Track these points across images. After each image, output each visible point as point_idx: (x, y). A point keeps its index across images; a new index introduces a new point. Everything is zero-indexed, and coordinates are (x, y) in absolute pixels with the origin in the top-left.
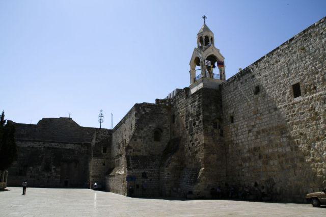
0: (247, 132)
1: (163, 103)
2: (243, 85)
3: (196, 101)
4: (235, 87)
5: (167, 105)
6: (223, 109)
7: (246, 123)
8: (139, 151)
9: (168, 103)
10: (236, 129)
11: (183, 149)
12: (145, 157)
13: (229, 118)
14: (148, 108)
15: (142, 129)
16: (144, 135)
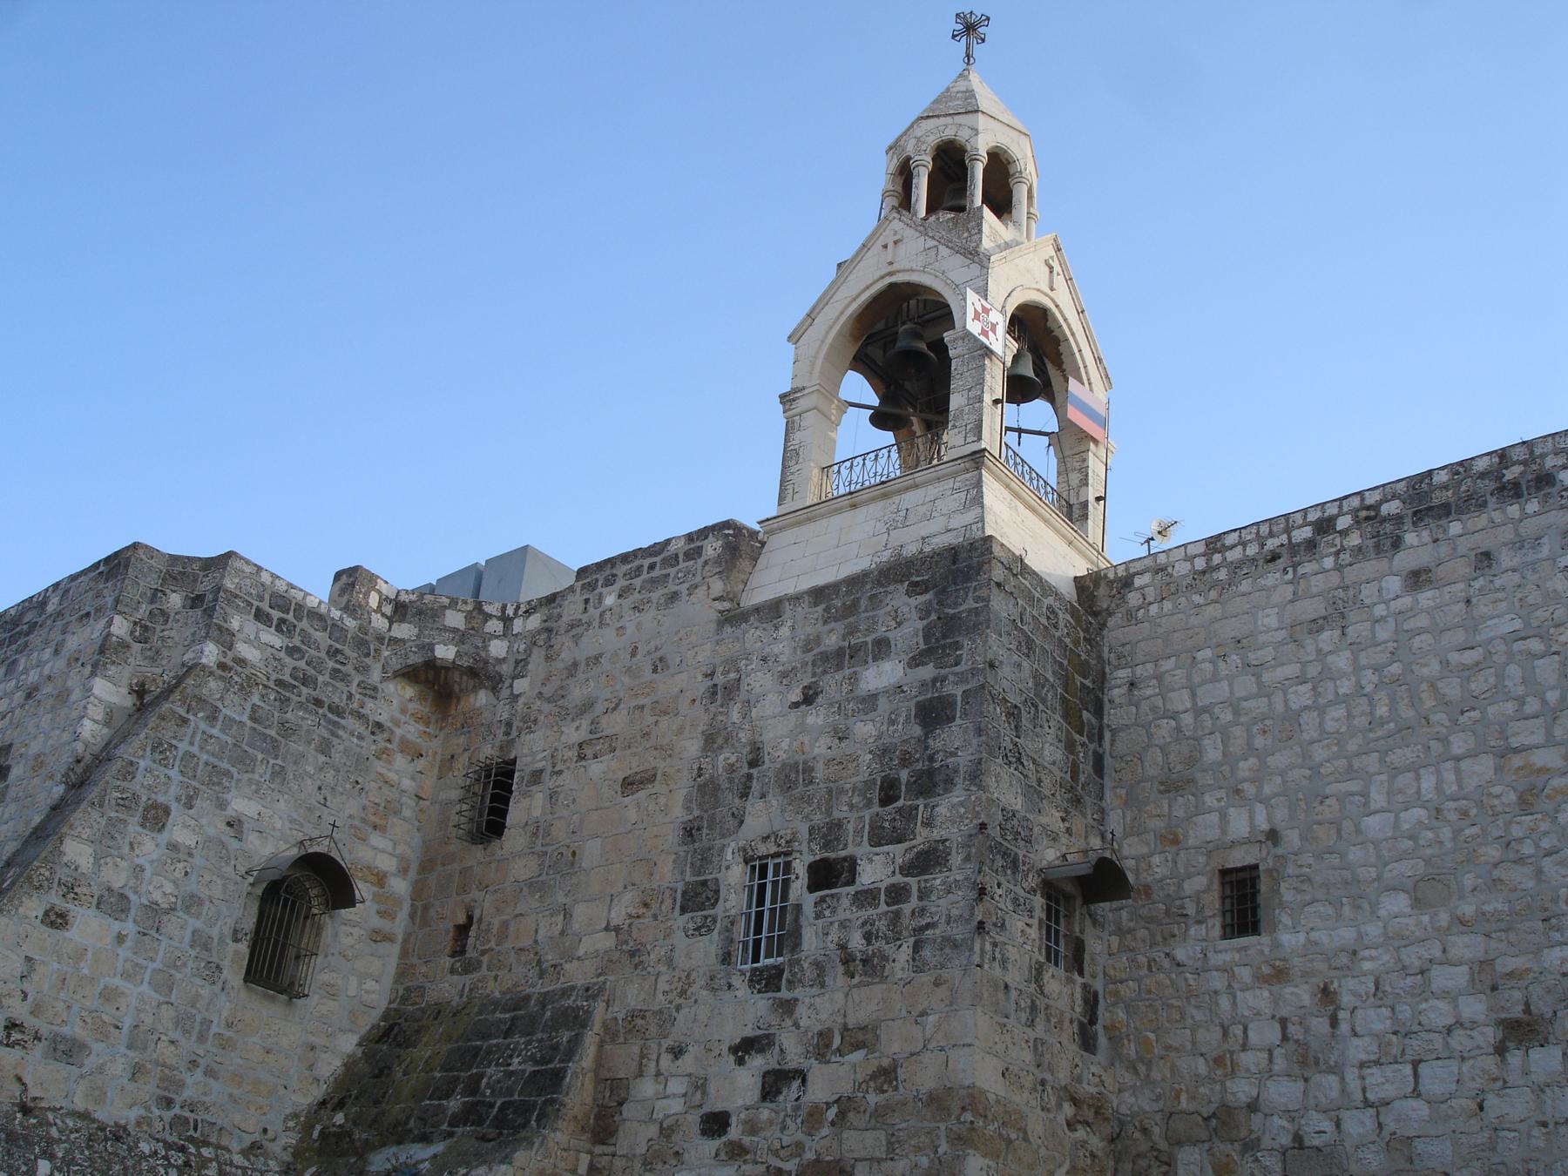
0: (1489, 1035)
1: (404, 631)
2: (1426, 598)
3: (882, 648)
4: (1313, 608)
5: (445, 652)
7: (1467, 946)
8: (67, 1051)
9: (460, 637)
10: (1300, 995)
11: (603, 1128)
12: (119, 1134)
13: (1199, 882)
14: (260, 616)
15: (156, 817)
16: (160, 890)
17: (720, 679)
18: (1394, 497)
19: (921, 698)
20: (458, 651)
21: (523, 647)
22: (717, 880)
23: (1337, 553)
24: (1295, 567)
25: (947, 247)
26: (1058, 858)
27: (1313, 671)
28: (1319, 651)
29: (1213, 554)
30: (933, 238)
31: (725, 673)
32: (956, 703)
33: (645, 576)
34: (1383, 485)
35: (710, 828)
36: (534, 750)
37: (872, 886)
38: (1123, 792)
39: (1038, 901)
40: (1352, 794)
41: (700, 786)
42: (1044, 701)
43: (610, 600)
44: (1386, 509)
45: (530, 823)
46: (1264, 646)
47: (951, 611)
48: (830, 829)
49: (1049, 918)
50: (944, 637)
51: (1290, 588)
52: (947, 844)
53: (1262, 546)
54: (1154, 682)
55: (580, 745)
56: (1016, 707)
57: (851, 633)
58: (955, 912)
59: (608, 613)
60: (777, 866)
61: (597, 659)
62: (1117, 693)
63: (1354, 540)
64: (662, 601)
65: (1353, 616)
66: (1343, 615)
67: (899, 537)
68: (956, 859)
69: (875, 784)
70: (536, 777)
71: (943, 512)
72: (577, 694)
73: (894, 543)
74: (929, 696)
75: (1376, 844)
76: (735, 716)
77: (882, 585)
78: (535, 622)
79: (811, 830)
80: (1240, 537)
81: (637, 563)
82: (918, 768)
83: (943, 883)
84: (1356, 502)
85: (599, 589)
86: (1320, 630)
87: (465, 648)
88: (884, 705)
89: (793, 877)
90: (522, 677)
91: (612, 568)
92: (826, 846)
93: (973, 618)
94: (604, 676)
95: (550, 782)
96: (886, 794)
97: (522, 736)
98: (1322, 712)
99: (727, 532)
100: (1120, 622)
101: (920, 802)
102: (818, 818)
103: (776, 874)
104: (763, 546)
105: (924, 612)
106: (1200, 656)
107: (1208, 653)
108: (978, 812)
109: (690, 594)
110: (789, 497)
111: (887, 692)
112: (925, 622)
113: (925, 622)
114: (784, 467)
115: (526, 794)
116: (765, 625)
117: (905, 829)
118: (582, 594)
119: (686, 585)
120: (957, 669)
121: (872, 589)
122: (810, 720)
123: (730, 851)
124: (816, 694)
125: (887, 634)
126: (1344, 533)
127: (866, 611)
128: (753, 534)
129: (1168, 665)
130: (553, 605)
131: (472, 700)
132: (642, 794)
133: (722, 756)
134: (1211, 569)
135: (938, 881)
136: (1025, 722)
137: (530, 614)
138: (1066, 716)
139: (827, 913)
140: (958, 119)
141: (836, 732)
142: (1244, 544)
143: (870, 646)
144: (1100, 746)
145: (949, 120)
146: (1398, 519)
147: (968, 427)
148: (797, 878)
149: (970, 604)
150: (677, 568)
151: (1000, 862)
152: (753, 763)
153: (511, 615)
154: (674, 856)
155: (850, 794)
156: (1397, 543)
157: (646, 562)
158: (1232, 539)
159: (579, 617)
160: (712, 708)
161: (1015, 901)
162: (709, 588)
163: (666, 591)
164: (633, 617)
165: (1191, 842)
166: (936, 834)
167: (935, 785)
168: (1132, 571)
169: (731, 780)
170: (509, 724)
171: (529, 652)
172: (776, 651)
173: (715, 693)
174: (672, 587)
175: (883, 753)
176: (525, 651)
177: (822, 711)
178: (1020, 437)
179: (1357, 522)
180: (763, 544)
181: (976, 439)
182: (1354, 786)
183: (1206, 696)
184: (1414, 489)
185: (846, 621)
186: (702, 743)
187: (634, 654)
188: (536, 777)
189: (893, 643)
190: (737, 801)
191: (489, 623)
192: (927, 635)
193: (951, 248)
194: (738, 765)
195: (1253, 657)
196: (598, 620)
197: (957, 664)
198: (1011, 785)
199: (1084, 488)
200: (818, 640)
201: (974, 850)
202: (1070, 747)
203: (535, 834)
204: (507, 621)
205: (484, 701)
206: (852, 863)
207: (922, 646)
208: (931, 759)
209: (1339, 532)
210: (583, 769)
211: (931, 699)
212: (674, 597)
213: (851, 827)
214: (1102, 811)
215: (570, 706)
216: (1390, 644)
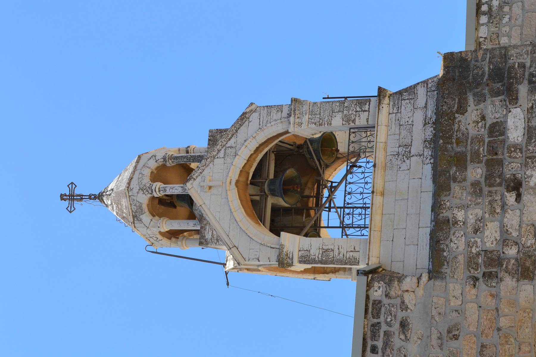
25: (230, 139)
30: (219, 151)
31: (477, 266)
67: (417, 147)
77: (452, 135)
109: (407, 308)
110: (356, 255)
111: (529, 119)
112: (488, 96)
113: (488, 96)
125: (487, 127)
134: (490, 13)
145: (137, 173)
147: (358, 109)
160: (501, 275)
162: (407, 291)
163: (397, 333)
172: (473, 221)
189: (495, 121)
197: (524, 67)
212: (404, 325)
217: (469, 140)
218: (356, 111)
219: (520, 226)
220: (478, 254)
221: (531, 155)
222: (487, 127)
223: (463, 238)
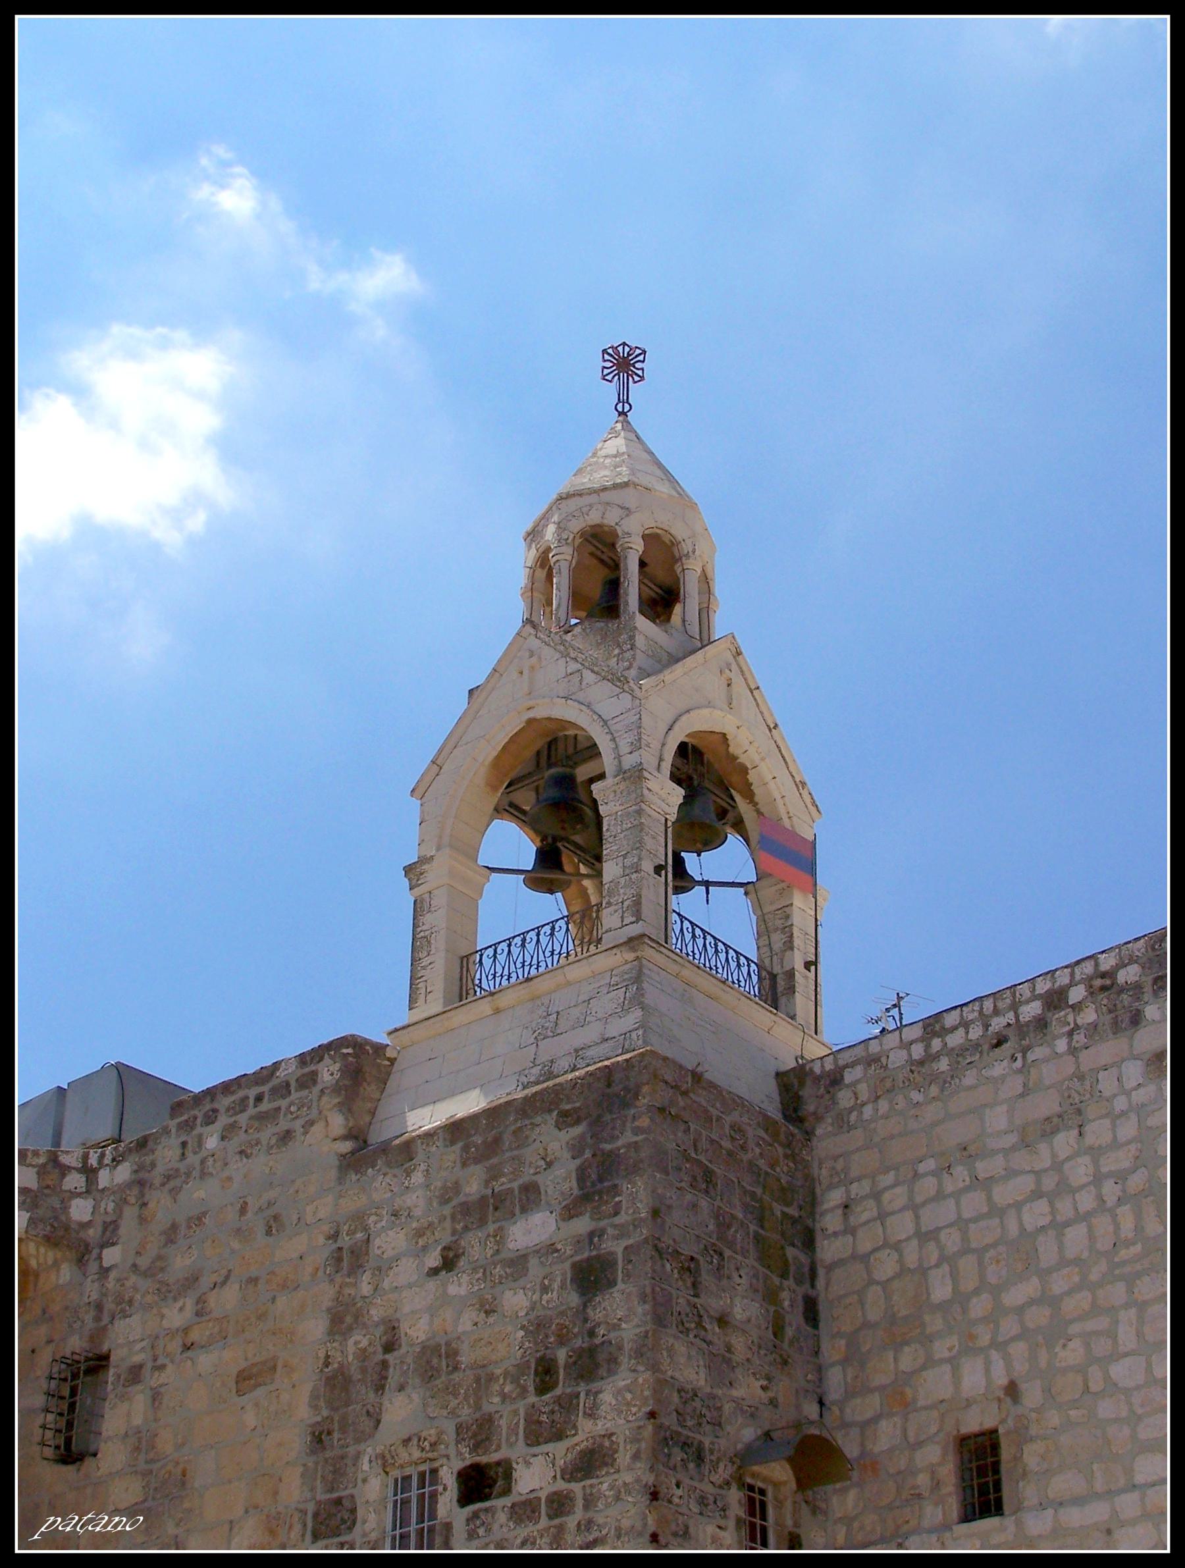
3: (530, 1196)
4: (1046, 1105)
6: (832, 1350)
13: (932, 1454)
17: (345, 1241)
18: (1132, 960)
19: (578, 1258)
20: (30, 1218)
21: (111, 1206)
22: (352, 1496)
23: (1070, 1034)
24: (1025, 1051)
25: (593, 671)
26: (757, 1439)
27: (1049, 1183)
28: (1054, 1156)
29: (931, 1039)
30: (575, 659)
31: (351, 1233)
32: (616, 1263)
33: (251, 1111)
34: (1119, 947)
35: (343, 1430)
36: (131, 1339)
37: (532, 1496)
38: (843, 1342)
39: (735, 1497)
40: (1097, 1333)
41: (328, 1379)
42: (731, 1245)
43: (212, 1143)
44: (1122, 977)
45: (130, 1433)
46: (994, 1152)
47: (607, 1147)
48: (480, 1426)
49: (752, 1513)
50: (601, 1180)
51: (1019, 1080)
52: (614, 1438)
53: (987, 1026)
54: (871, 1203)
55: (186, 1330)
56: (692, 1259)
57: (495, 1178)
58: (626, 1523)
59: (211, 1159)
60: (422, 1475)
61: (199, 1219)
62: (831, 1221)
63: (1089, 1016)
64: (273, 1141)
65: (1091, 1111)
66: (1079, 1112)
67: (551, 1049)
68: (623, 1457)
69: (529, 1368)
70: (135, 1374)
71: (599, 1015)
72: (180, 1263)
73: (543, 1058)
74: (586, 1255)
75: (1127, 1392)
76: (366, 1289)
78: (124, 1173)
79: (459, 1428)
80: (961, 1015)
81: (241, 1094)
82: (577, 1345)
83: (611, 1488)
84: (1088, 968)
85: (199, 1130)
86: (1055, 1131)
87: (41, 1212)
88: (535, 1269)
89: (440, 1488)
90: (113, 1244)
91: (212, 1100)
92: (476, 1448)
93: (633, 1154)
94: (210, 1241)
95: (153, 1380)
96: (542, 1381)
97: (116, 1322)
98: (1060, 1235)
99: (345, 1051)
100: (830, 1129)
101: (582, 1388)
102: (466, 1413)
103: (422, 1485)
104: (392, 1064)
105: (576, 1149)
106: (922, 1168)
107: (931, 1164)
108: (646, 1398)
111: (538, 1252)
112: (578, 1162)
114: (414, 960)
115: (122, 1397)
116: (396, 1171)
117: (565, 1422)
118: (178, 1136)
119: (300, 1122)
120: (617, 1220)
121: (516, 1121)
122: (453, 1290)
123: (366, 1459)
124: (457, 1256)
126: (1077, 1008)
127: (511, 1149)
128: (379, 1049)
129: (888, 1179)
130: (144, 1151)
131: (53, 1277)
132: (260, 1392)
133: (351, 1342)
134: (930, 1057)
135: (605, 1486)
136: (706, 1278)
137: (119, 1162)
138: (764, 1256)
139: (481, 1531)
140: (605, 496)
141: (482, 1306)
142: (965, 1024)
143: (516, 1192)
144: (813, 1286)
145: (593, 498)
146: (1137, 988)
147: (626, 904)
148: (445, 1489)
149: (628, 1137)
150: (288, 1100)
151: (678, 1455)
152: (389, 1347)
153: (95, 1164)
154: (301, 1469)
155: (501, 1381)
156: (1136, 1019)
157: (252, 1093)
158: (951, 1020)
159: (177, 1165)
160: (338, 1279)
161: (702, 1501)
164: (240, 1165)
165: (921, 1403)
166: (600, 1427)
167: (597, 1366)
168: (841, 1063)
169: (363, 1370)
170: (99, 1307)
171: (119, 1211)
172: (409, 1203)
173: (339, 1260)
174: (284, 1124)
175: (537, 1327)
176: (114, 1210)
177: (465, 1278)
178: (708, 893)
179: (1092, 993)
180: (392, 1061)
181: (634, 919)
182: (1102, 1323)
183: (933, 1216)
184: (1153, 949)
185: (488, 1164)
186: (327, 1323)
187: (243, 1210)
188: (135, 1374)
190: (371, 1395)
191: (68, 1179)
192: (582, 1175)
193: (597, 673)
194: (371, 1350)
195: (983, 1168)
196: (198, 1168)
197: (616, 1214)
198: (689, 1357)
199: (788, 953)
200: (457, 1188)
201: (643, 1445)
202: (771, 1297)
203: (137, 1449)
204: (90, 1172)
205: (68, 1277)
206: (506, 1469)
207: (576, 1192)
208: (592, 1333)
209: (1072, 1007)
210: (189, 1363)
211: (588, 1259)
213: (503, 1422)
214: (819, 1369)
215: (171, 1281)
216: (1133, 1147)
217: (516, 1153)
218: (622, 902)
219: (396, 1287)
220: (366, 1229)
221: (488, 1273)
222: (535, 1178)
223: (389, 1194)
